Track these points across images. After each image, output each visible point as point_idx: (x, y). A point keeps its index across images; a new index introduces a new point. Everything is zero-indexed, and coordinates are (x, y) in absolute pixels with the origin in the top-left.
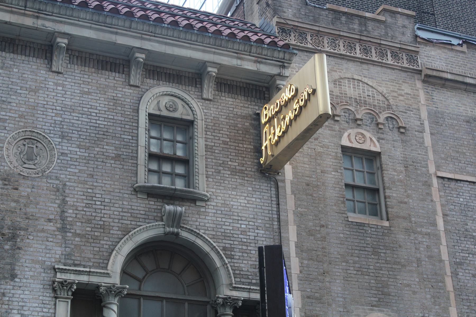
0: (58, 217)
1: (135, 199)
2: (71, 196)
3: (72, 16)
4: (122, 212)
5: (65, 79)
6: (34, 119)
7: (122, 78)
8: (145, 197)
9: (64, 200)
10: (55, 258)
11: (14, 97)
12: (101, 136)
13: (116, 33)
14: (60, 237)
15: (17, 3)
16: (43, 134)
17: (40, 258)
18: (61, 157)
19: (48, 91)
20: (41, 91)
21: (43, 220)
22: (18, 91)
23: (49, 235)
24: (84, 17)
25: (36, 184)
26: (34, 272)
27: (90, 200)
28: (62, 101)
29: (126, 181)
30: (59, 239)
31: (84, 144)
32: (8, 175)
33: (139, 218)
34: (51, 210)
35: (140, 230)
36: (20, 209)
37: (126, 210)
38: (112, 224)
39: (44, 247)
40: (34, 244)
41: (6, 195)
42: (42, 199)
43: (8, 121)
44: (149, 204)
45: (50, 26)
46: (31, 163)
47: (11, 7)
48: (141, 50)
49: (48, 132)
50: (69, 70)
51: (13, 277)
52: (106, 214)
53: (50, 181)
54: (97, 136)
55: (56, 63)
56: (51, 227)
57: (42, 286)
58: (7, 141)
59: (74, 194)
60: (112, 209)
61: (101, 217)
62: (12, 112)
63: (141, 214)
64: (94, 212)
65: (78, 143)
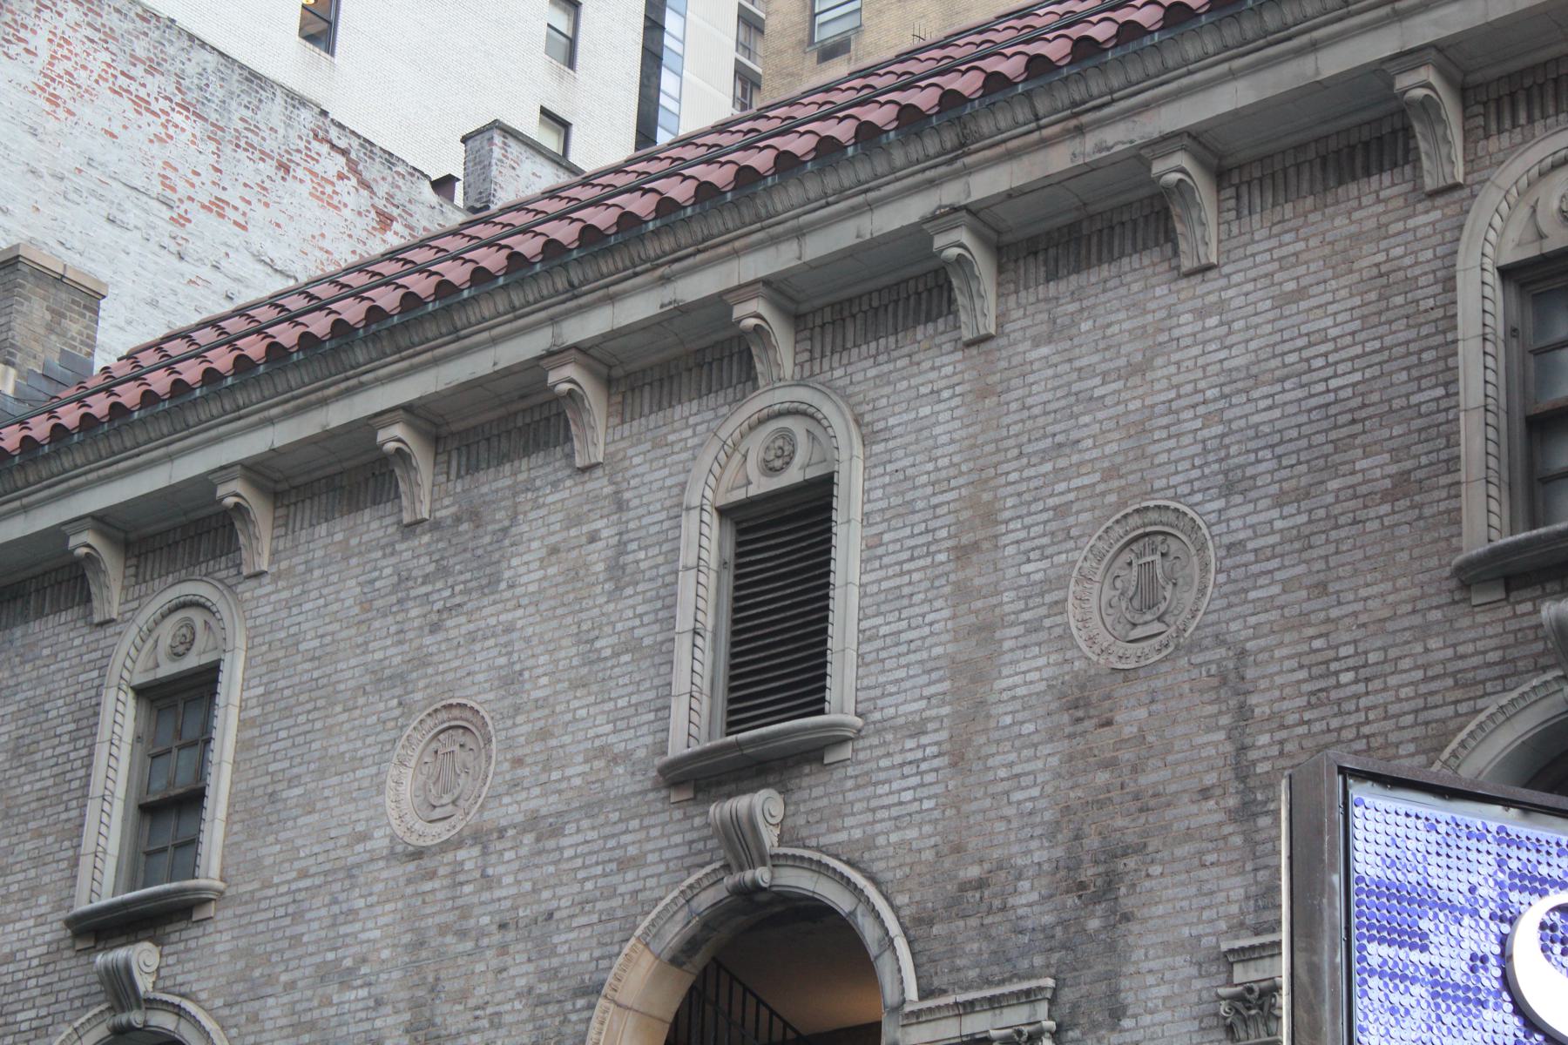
0: (1230, 774)
1: (1464, 615)
2: (1263, 684)
3: (1167, 70)
4: (1426, 680)
5: (1223, 282)
6: (1145, 464)
7: (1404, 182)
8: (1500, 594)
9: (1241, 707)
10: (1228, 917)
11: (1086, 419)
12: (1345, 431)
13: (1314, 47)
14: (1237, 840)
15: (1010, 121)
16: (1173, 505)
17: (1186, 931)
18: (1228, 562)
19: (1179, 349)
20: (1159, 361)
21: (1186, 798)
22: (1097, 393)
23: (1204, 845)
24: (1200, 52)
25: (1159, 683)
26: (1172, 982)
27: (1321, 676)
28: (1221, 361)
29: (1434, 562)
30: (1237, 848)
31: (1294, 482)
32: (1082, 687)
33: (1483, 682)
34: (1209, 757)
35: (1480, 726)
36: (1122, 788)
37: (1439, 669)
38: (1393, 738)
39: (1193, 890)
40: (1166, 888)
41: (1083, 752)
42: (1180, 730)
43: (1075, 508)
44: (1515, 616)
45: (1118, 137)
46: (1148, 617)
47: (1004, 141)
48: (1408, 58)
49: (1185, 489)
50: (1234, 242)
51: (1116, 1013)
52: (1375, 707)
53: (1197, 659)
54: (1333, 435)
55: (1186, 238)
56: (1209, 814)
57: (1195, 1025)
58: (1075, 573)
59: (1272, 675)
60: (1393, 681)
61: (1359, 725)
62: (1083, 471)
63: (1489, 665)
64: (1335, 715)
65: (1274, 489)
